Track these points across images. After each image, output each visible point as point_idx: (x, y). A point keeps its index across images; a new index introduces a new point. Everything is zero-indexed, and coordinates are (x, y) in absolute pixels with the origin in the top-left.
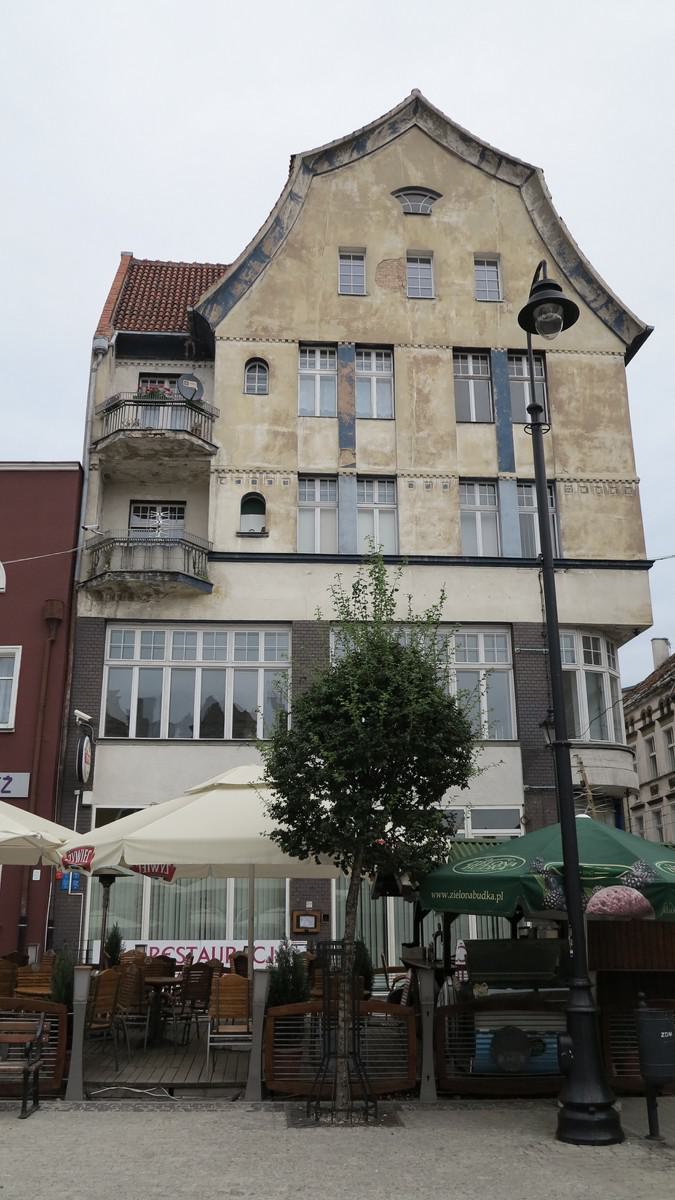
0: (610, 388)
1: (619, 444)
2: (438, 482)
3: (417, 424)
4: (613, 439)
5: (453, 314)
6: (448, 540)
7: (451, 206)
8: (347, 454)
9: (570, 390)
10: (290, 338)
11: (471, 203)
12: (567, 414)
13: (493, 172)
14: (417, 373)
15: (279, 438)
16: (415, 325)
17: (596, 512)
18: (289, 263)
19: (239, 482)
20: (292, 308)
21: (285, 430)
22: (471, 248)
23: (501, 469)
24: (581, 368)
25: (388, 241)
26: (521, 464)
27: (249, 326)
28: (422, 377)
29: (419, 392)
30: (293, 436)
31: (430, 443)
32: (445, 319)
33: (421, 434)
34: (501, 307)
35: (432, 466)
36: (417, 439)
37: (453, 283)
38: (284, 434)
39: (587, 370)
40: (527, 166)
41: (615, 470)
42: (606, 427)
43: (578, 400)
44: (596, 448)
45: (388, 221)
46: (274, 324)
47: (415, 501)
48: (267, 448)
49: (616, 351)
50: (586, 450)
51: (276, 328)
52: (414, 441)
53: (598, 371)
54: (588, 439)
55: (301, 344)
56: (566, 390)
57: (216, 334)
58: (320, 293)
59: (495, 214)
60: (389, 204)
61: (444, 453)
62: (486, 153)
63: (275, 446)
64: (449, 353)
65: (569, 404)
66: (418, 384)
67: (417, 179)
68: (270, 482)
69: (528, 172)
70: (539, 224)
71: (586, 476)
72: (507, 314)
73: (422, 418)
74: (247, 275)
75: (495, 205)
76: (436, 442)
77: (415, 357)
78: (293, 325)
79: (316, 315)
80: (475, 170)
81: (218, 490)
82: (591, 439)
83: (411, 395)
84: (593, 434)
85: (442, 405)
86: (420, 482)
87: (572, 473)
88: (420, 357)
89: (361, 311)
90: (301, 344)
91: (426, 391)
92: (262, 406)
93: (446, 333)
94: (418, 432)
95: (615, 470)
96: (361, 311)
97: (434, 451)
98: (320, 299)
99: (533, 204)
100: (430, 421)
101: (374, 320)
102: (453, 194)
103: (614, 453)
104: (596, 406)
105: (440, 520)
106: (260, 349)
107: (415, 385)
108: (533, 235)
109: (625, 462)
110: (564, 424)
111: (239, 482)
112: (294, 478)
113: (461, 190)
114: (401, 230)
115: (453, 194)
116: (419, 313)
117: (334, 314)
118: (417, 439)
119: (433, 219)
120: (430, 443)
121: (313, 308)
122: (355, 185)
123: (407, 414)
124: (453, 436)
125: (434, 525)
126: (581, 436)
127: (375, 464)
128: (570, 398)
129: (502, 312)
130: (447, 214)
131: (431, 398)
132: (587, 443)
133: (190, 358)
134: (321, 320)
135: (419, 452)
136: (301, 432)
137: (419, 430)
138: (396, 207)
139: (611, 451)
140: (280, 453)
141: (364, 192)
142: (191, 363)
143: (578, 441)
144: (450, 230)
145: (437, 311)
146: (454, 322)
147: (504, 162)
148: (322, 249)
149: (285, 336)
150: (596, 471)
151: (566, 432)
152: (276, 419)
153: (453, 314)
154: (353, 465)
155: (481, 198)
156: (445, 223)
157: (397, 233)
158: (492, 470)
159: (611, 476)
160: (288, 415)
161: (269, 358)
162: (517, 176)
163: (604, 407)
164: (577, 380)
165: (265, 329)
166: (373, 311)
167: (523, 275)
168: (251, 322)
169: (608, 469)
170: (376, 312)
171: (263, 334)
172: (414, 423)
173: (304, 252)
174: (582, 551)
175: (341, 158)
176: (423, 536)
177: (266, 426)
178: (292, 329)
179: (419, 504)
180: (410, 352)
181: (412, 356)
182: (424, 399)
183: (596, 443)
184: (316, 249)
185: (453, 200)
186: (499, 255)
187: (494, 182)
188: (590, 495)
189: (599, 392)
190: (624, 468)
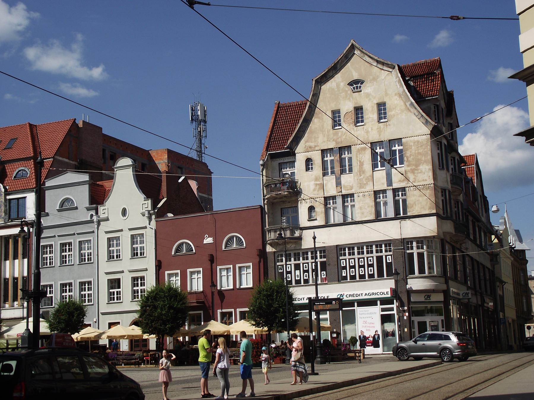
0: (425, 149)
1: (427, 170)
3: (360, 174)
4: (425, 168)
5: (370, 130)
6: (371, 214)
7: (368, 85)
9: (410, 152)
10: (318, 150)
11: (375, 82)
14: (359, 154)
15: (317, 186)
17: (419, 197)
19: (307, 203)
20: (318, 138)
21: (319, 183)
23: (388, 186)
24: (414, 143)
26: (395, 183)
27: (305, 147)
28: (361, 156)
29: (360, 161)
31: (364, 180)
32: (367, 132)
33: (361, 177)
34: (386, 124)
35: (365, 188)
37: (370, 117)
38: (319, 184)
39: (416, 143)
41: (426, 180)
42: (423, 164)
43: (413, 156)
44: (420, 173)
46: (312, 144)
47: (360, 201)
48: (314, 190)
49: (427, 134)
50: (416, 174)
51: (313, 146)
52: (359, 180)
53: (420, 142)
54: (416, 170)
56: (409, 152)
58: (327, 129)
59: (383, 85)
60: (347, 89)
61: (368, 183)
63: (316, 189)
65: (410, 157)
66: (360, 159)
67: (356, 77)
72: (389, 126)
73: (362, 171)
74: (302, 128)
75: (383, 81)
76: (366, 179)
77: (358, 149)
78: (319, 144)
79: (326, 139)
83: (358, 163)
84: (419, 168)
88: (360, 148)
91: (362, 161)
93: (368, 138)
94: (360, 176)
95: (426, 180)
96: (340, 134)
100: (364, 172)
102: (369, 80)
103: (425, 174)
104: (420, 157)
105: (368, 207)
107: (359, 159)
109: (429, 176)
110: (408, 166)
113: (371, 77)
114: (351, 99)
115: (369, 80)
116: (359, 132)
117: (331, 137)
118: (360, 179)
119: (362, 92)
120: (364, 180)
121: (324, 136)
122: (335, 84)
123: (356, 171)
125: (366, 209)
127: (348, 190)
128: (411, 155)
129: (386, 126)
131: (364, 163)
132: (416, 172)
134: (327, 141)
135: (361, 184)
137: (361, 176)
139: (424, 173)
140: (318, 191)
141: (338, 85)
143: (413, 171)
144: (368, 95)
145: (365, 130)
146: (371, 133)
149: (317, 148)
150: (419, 182)
151: (409, 168)
152: (316, 179)
153: (370, 130)
154: (341, 192)
155: (379, 79)
156: (366, 93)
157: (350, 101)
158: (385, 187)
159: (425, 183)
160: (319, 177)
163: (422, 156)
164: (413, 148)
165: (310, 147)
166: (344, 134)
167: (393, 109)
168: (306, 146)
169: (423, 180)
170: (345, 134)
171: (309, 149)
172: (359, 173)
174: (414, 212)
175: (329, 74)
176: (363, 213)
177: (313, 182)
178: (318, 146)
179: (361, 202)
180: (356, 147)
181: (357, 148)
182: (361, 164)
183: (419, 171)
185: (369, 82)
186: (385, 102)
187: (383, 71)
189: (421, 151)
190: (429, 179)
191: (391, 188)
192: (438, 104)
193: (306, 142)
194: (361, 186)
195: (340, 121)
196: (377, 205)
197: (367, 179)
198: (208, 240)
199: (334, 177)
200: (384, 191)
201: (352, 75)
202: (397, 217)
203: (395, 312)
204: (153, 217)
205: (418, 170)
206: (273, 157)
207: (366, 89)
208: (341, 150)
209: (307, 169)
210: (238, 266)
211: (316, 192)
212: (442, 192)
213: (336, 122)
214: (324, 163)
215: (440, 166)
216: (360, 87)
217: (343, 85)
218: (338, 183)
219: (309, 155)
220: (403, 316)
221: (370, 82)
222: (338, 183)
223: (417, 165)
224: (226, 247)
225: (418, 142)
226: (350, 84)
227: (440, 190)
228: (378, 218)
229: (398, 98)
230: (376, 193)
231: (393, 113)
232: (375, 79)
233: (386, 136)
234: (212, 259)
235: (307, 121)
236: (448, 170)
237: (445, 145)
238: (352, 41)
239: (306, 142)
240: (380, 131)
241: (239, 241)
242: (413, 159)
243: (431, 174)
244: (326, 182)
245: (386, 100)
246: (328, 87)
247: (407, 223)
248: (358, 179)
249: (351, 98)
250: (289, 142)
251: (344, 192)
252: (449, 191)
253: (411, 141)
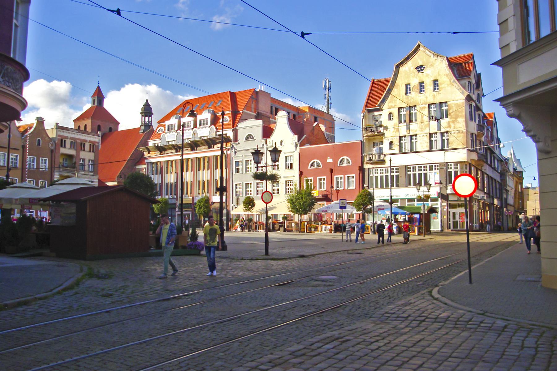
1: (462, 121)
2: (425, 135)
6: (427, 147)
8: (408, 131)
12: (452, 116)
16: (420, 100)
23: (438, 130)
24: (455, 105)
25: (414, 82)
31: (423, 126)
41: (461, 128)
45: (414, 76)
46: (393, 105)
48: (393, 132)
50: (455, 124)
60: (415, 71)
71: (454, 130)
76: (425, 126)
84: (457, 120)
86: (421, 135)
87: (452, 129)
95: (461, 128)
96: (410, 98)
97: (424, 128)
101: (412, 100)
110: (451, 118)
113: (430, 64)
120: (423, 126)
132: (455, 122)
138: (416, 71)
141: (409, 69)
143: (453, 122)
144: (427, 75)
148: (401, 85)
150: (457, 128)
151: (451, 120)
154: (410, 133)
158: (436, 131)
164: (454, 107)
169: (460, 128)
183: (457, 122)
184: (400, 86)
188: (455, 134)
191: (440, 131)
192: (471, 81)
193: (389, 103)
194: (422, 130)
195: (410, 90)
196: (431, 142)
197: (426, 126)
198: (330, 160)
199: (405, 124)
200: (436, 133)
201: (418, 63)
202: (443, 149)
203: (439, 206)
204: (298, 145)
205: (456, 121)
206: (369, 111)
207: (427, 71)
208: (410, 107)
209: (390, 119)
210: (346, 176)
211: (394, 133)
212: (471, 135)
213: (408, 91)
214: (400, 116)
215: (470, 119)
216: (423, 70)
217: (413, 68)
218: (408, 128)
219: (391, 111)
220: (444, 209)
222: (408, 128)
223: (456, 118)
224: (340, 164)
225: (457, 104)
226: (417, 68)
227: (470, 134)
228: (431, 149)
229: (446, 77)
230: (431, 135)
232: (432, 65)
233: (438, 101)
234: (332, 171)
235: (390, 90)
236: (475, 121)
237: (474, 106)
238: (419, 42)
239: (389, 103)
240: (434, 97)
241: (348, 162)
242: (454, 114)
243: (464, 124)
245: (439, 78)
246: (403, 70)
247: (448, 153)
250: (379, 103)
251: (411, 134)
252: (475, 135)
253: (453, 103)
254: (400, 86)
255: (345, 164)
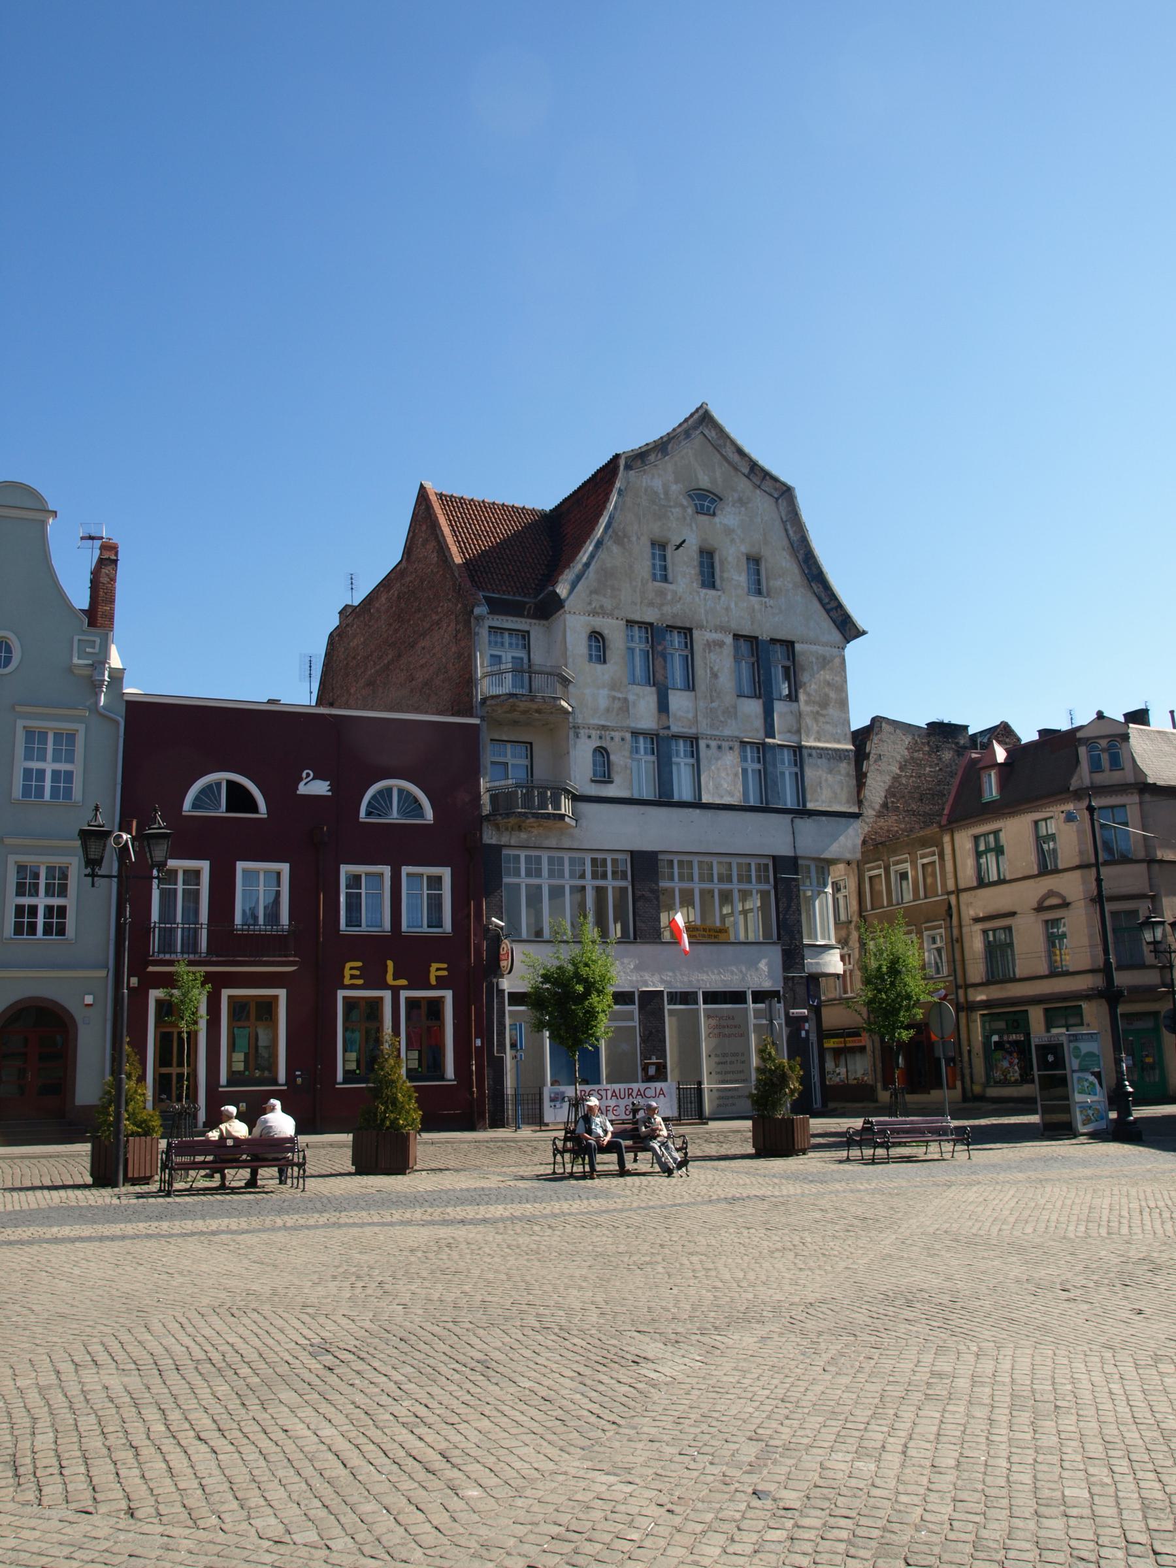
2: (725, 745)
5: (733, 605)
11: (743, 509)
12: (808, 695)
13: (758, 483)
15: (616, 702)
18: (615, 549)
19: (589, 737)
21: (620, 695)
22: (744, 549)
29: (711, 669)
30: (626, 700)
32: (727, 609)
33: (713, 704)
36: (711, 709)
38: (619, 699)
39: (821, 660)
40: (784, 484)
46: (608, 604)
48: (608, 710)
51: (609, 607)
55: (627, 621)
57: (566, 608)
60: (685, 503)
62: (754, 467)
64: (731, 636)
68: (612, 738)
69: (785, 488)
70: (791, 532)
76: (724, 713)
80: (745, 479)
81: (575, 744)
82: (823, 716)
85: (726, 681)
86: (713, 744)
89: (669, 597)
90: (627, 621)
91: (716, 669)
92: (603, 674)
97: (722, 719)
98: (640, 584)
99: (786, 515)
106: (599, 623)
108: (785, 543)
110: (807, 703)
111: (589, 737)
112: (628, 736)
113: (736, 496)
119: (717, 520)
124: (735, 707)
126: (818, 712)
130: (728, 517)
131: (719, 674)
132: (821, 719)
133: (528, 617)
136: (631, 698)
140: (618, 715)
142: (529, 621)
143: (816, 716)
144: (729, 531)
147: (768, 478)
148: (638, 538)
152: (613, 686)
153: (733, 605)
154: (668, 728)
155: (750, 505)
161: (606, 632)
162: (776, 489)
165: (602, 607)
173: (626, 540)
188: (824, 760)
218: (663, 707)
221: (733, 506)
222: (663, 707)
231: (778, 583)
241: (411, 805)
244: (635, 697)
248: (706, 708)
249: (694, 525)
254: (634, 539)
255: (395, 816)
